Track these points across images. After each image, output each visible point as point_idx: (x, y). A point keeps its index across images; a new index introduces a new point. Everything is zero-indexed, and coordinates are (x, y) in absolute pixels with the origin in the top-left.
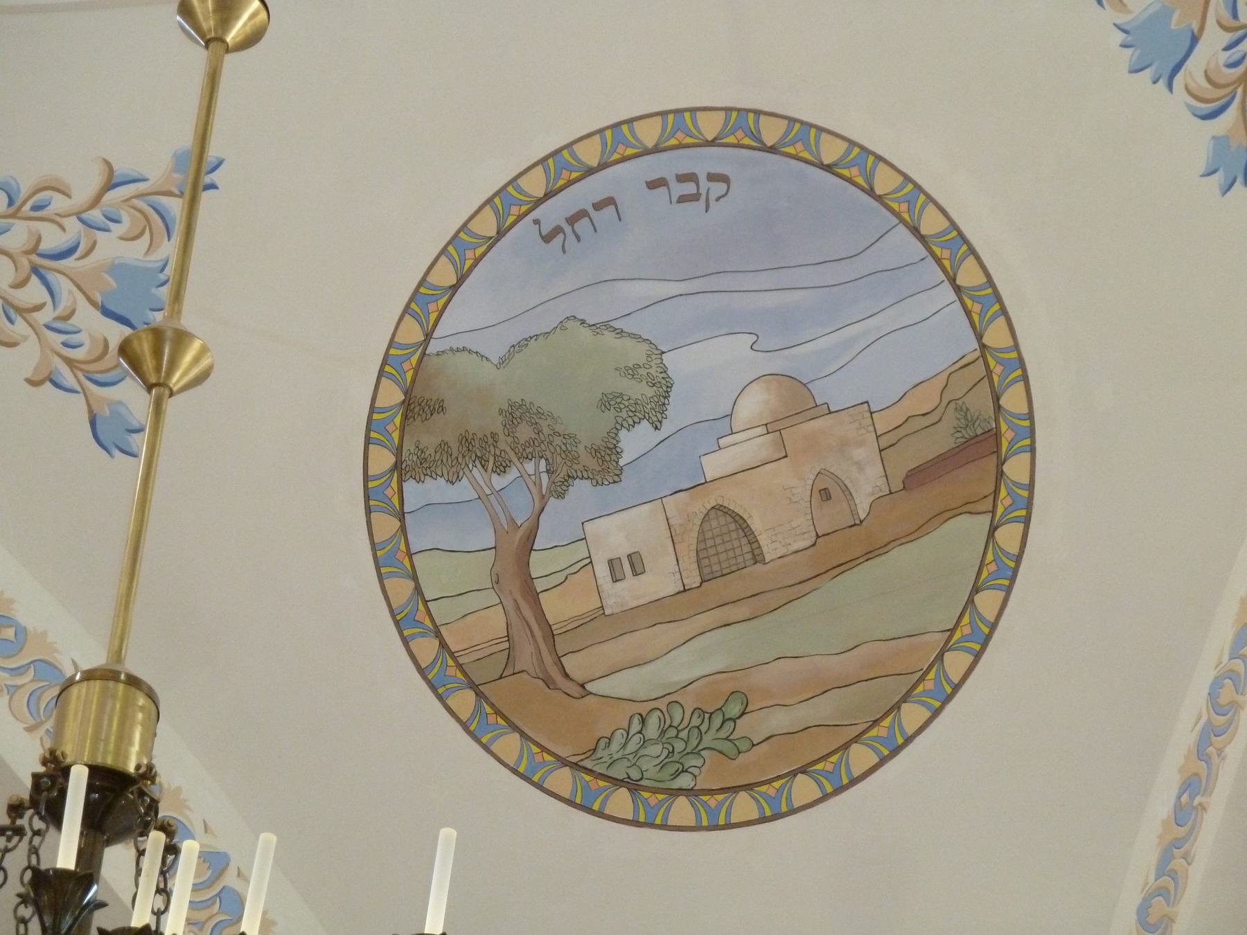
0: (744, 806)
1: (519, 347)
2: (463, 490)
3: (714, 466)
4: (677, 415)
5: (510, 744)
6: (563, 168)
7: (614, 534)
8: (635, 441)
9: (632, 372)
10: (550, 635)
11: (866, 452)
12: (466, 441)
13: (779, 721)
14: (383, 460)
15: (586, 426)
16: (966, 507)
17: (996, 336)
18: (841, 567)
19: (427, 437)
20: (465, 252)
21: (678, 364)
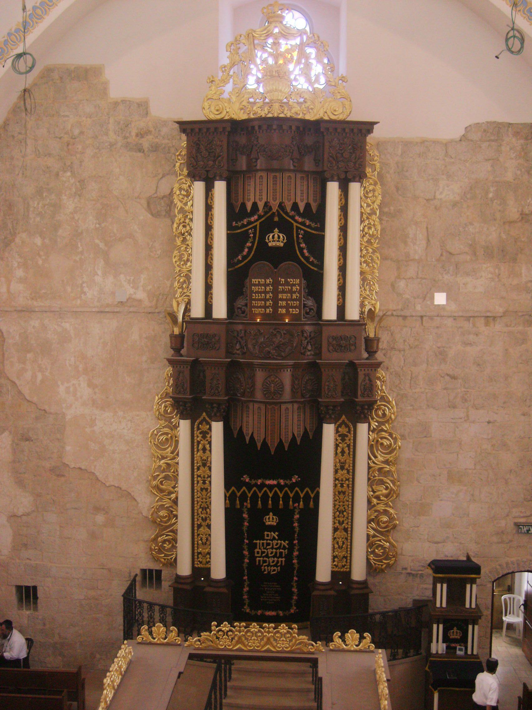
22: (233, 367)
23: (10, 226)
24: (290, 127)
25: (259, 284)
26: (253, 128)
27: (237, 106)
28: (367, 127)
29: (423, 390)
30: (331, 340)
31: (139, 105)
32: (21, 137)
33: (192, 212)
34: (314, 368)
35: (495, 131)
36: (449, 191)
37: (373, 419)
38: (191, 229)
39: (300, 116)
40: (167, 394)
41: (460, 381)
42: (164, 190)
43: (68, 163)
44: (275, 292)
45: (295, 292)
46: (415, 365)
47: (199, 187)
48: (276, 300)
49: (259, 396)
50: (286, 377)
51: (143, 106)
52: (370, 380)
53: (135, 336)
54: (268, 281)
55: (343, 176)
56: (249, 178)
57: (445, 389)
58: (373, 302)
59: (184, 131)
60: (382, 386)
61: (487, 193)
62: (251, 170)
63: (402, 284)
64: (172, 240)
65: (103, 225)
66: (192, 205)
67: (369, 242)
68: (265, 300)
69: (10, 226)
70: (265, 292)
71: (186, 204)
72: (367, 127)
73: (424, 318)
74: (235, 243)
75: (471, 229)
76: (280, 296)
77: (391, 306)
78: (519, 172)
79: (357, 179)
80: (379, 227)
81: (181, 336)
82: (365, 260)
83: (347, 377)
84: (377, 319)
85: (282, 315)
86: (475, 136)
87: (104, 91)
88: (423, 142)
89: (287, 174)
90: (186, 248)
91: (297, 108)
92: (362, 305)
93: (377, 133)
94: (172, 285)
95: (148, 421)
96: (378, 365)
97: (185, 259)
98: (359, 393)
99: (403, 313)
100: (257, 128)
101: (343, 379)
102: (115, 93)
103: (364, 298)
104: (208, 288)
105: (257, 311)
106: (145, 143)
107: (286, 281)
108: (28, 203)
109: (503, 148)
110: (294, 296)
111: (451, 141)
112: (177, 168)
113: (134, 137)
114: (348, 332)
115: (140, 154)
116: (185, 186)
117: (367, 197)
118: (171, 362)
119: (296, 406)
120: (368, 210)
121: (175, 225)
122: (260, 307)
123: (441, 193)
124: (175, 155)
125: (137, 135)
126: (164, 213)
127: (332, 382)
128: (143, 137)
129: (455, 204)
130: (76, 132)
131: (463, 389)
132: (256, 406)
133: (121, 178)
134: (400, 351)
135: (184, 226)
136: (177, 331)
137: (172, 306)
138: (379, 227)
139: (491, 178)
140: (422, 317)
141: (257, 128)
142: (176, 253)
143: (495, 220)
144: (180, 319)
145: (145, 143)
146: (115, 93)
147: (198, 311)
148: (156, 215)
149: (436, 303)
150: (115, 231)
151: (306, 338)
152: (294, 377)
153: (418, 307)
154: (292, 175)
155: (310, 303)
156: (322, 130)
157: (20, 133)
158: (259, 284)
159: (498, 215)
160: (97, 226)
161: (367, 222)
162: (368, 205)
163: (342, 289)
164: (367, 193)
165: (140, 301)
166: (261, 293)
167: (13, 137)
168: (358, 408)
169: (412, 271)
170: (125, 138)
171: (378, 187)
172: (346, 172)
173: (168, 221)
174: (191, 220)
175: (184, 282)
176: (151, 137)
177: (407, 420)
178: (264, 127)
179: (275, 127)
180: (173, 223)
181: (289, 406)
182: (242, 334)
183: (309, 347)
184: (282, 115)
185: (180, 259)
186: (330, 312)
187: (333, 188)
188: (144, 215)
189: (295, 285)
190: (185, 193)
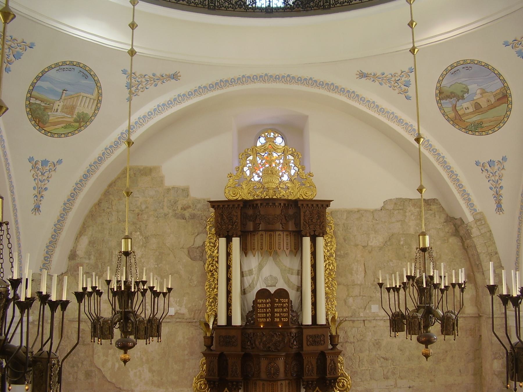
0: (484, 133)
1: (451, 86)
2: (447, 101)
3: (475, 98)
4: (470, 93)
5: (457, 126)
6: (452, 66)
7: (465, 105)
8: (466, 95)
9: (464, 88)
10: (460, 116)
11: (492, 97)
12: (447, 96)
13: (486, 125)
14: (438, 99)
15: (460, 94)
16: (505, 103)
17: (505, 85)
18: (492, 109)
19: (443, 96)
20: (443, 76)
21: (469, 87)
22: (246, 358)
23: (100, 266)
24: (280, 204)
25: (262, 303)
26: (257, 205)
27: (246, 191)
28: (326, 203)
29: (367, 368)
30: (309, 338)
31: (183, 190)
32: (108, 210)
33: (218, 257)
34: (299, 357)
35: (400, 204)
36: (376, 241)
37: (336, 388)
38: (217, 268)
39: (286, 197)
40: (201, 377)
41: (390, 361)
42: (199, 242)
43: (138, 226)
45: (285, 308)
46: (361, 351)
47: (223, 241)
48: (273, 313)
49: (263, 376)
50: (281, 363)
51: (185, 191)
52: (335, 364)
53: (180, 338)
54: (268, 301)
55: (312, 234)
56: (254, 235)
57: (381, 367)
58: (334, 312)
59: (213, 207)
60: (341, 366)
61: (399, 241)
62: (256, 230)
63: (351, 300)
64: (204, 275)
65: (160, 265)
66: (218, 253)
67: (329, 273)
68: (266, 313)
69: (100, 266)
70: (266, 308)
71: (213, 252)
72: (326, 203)
73: (366, 322)
75: (391, 264)
76: (276, 310)
77: (345, 314)
78: (417, 228)
79: (321, 235)
80: (335, 265)
81: (212, 337)
82: (328, 285)
83: (319, 361)
84: (337, 324)
85: (277, 322)
86: (390, 207)
87: (162, 182)
88: (358, 211)
89: (278, 233)
90: (214, 280)
91: (283, 192)
92: (327, 315)
93: (333, 206)
94: (204, 304)
96: (339, 353)
97: (213, 287)
98: (328, 372)
99: (352, 319)
100: (259, 205)
101: (317, 363)
103: (328, 310)
104: (229, 305)
105: (261, 320)
106: (187, 214)
107: (279, 300)
108: (112, 252)
109: (407, 214)
110: (285, 310)
111: (376, 210)
112: (207, 229)
113: (180, 210)
114: (319, 332)
115: (183, 221)
116: (213, 241)
117: (327, 246)
118: (205, 354)
119: (287, 382)
120: (328, 254)
121: (206, 266)
122: (263, 318)
123: (371, 242)
124: (206, 221)
125: (182, 209)
126: (199, 258)
127: (310, 364)
128: (185, 210)
129: (381, 249)
130: (143, 207)
131: (392, 366)
132: (261, 383)
133: (172, 236)
134: (351, 343)
135: (212, 266)
136: (208, 335)
137: (204, 318)
138: (335, 265)
139: (401, 232)
140: (364, 321)
141: (259, 205)
142: (207, 283)
143: (405, 258)
144: (211, 327)
145: (187, 214)
146: (169, 183)
147: (222, 321)
148: (193, 259)
149: (373, 311)
150: (167, 269)
151: (293, 337)
152: (286, 363)
153: (362, 314)
154: (281, 233)
156: (299, 205)
157: (108, 208)
158: (262, 303)
159: (407, 255)
160: (156, 266)
161: (327, 262)
162: (328, 251)
163: (314, 304)
164: (327, 243)
165: (183, 314)
166: (263, 308)
167: (104, 210)
168: (328, 382)
169: (356, 291)
170: (174, 210)
171: (334, 239)
172: (315, 231)
174: (217, 262)
175: (213, 302)
176: (190, 210)
177: (358, 388)
178: (265, 204)
179: (271, 204)
180: (205, 264)
181: (283, 382)
182: (252, 336)
183: (295, 343)
184: (275, 197)
185: (210, 288)
187: (307, 241)
188: (186, 259)
189: (285, 303)
190: (213, 245)
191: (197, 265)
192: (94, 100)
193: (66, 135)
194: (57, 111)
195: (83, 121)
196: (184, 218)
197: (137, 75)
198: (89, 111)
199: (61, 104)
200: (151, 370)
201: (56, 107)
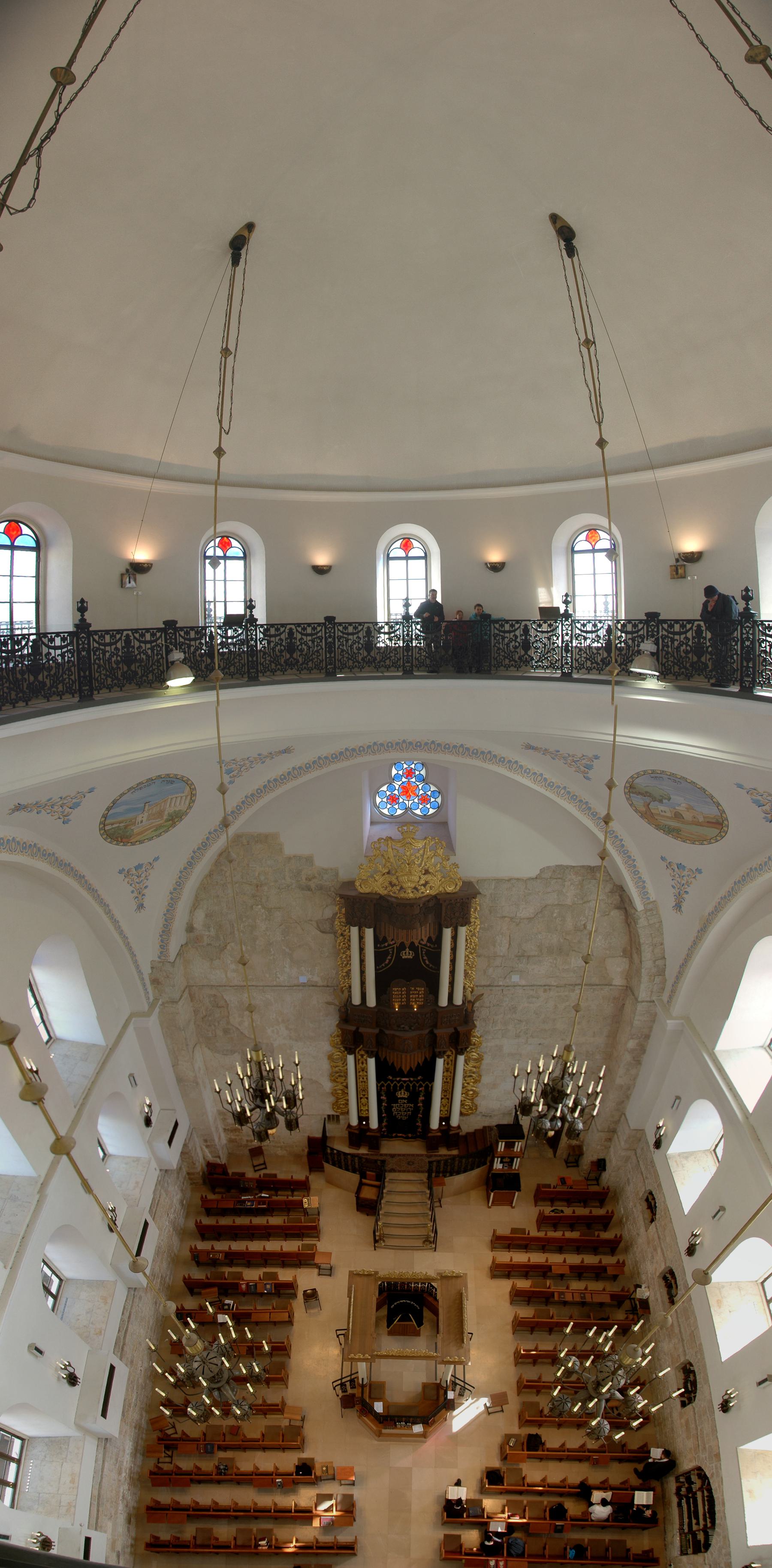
44: (408, 994)
47: (354, 931)
51: (309, 860)
74: (379, 958)
88: (509, 880)
95: (325, 1047)
102: (288, 851)
104: (363, 983)
115: (309, 892)
128: (310, 880)
129: (530, 919)
145: (312, 884)
147: (356, 1000)
155: (431, 997)
173: (332, 935)
174: (349, 940)
186: (443, 1002)
187: (447, 933)
191: (329, 938)
192: (186, 797)
193: (159, 835)
194: (142, 822)
195: (175, 818)
196: (309, 889)
197: (238, 760)
198: (183, 807)
199: (146, 815)
200: (287, 1028)
201: (139, 819)
